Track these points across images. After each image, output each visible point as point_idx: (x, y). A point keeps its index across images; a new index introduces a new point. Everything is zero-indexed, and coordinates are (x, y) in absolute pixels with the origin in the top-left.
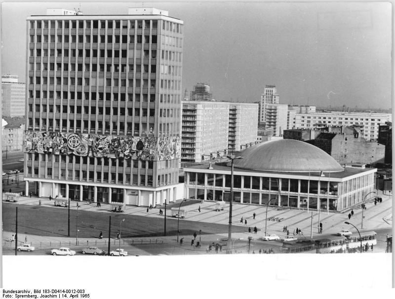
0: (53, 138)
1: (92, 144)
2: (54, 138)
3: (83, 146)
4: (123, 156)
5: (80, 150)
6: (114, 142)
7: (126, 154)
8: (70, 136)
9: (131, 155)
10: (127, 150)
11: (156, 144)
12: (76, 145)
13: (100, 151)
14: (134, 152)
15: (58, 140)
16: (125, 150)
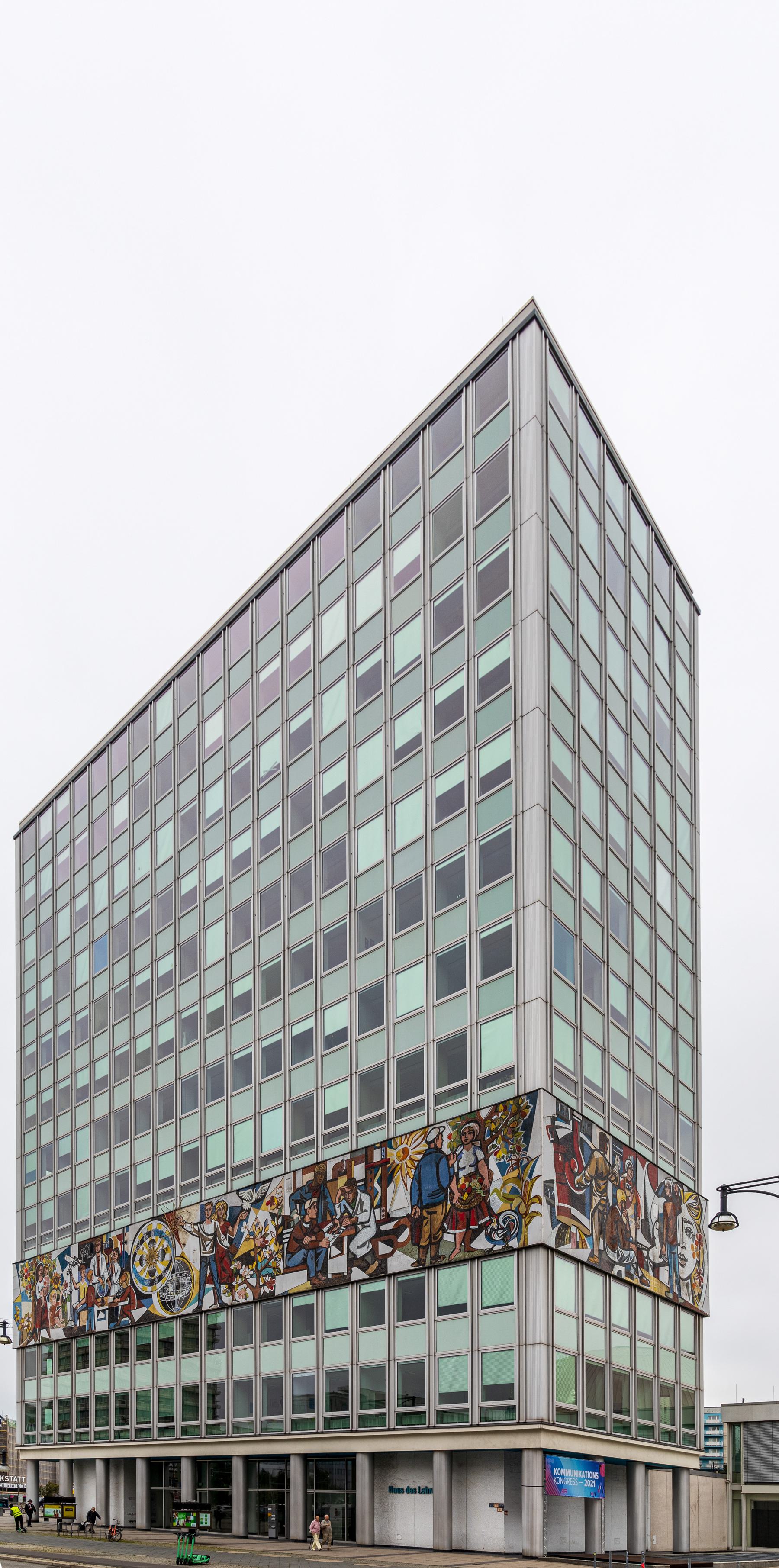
0: (87, 1265)
1: (215, 1244)
2: (94, 1260)
3: (184, 1266)
4: (343, 1270)
5: (172, 1288)
6: (302, 1202)
7: (360, 1253)
8: (137, 1241)
9: (383, 1249)
10: (365, 1224)
11: (527, 1138)
12: (157, 1274)
13: (246, 1271)
14: (397, 1231)
15: (104, 1267)
16: (354, 1228)
